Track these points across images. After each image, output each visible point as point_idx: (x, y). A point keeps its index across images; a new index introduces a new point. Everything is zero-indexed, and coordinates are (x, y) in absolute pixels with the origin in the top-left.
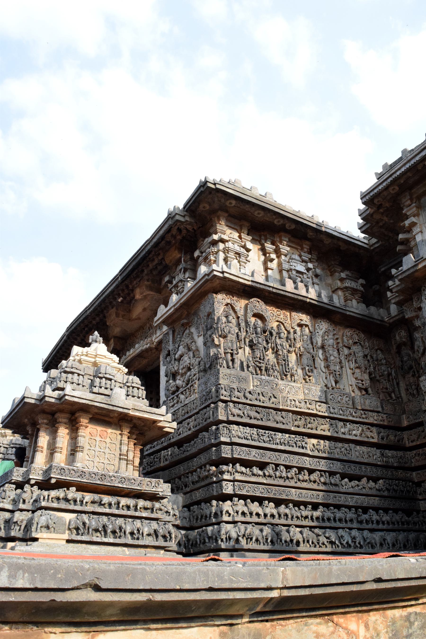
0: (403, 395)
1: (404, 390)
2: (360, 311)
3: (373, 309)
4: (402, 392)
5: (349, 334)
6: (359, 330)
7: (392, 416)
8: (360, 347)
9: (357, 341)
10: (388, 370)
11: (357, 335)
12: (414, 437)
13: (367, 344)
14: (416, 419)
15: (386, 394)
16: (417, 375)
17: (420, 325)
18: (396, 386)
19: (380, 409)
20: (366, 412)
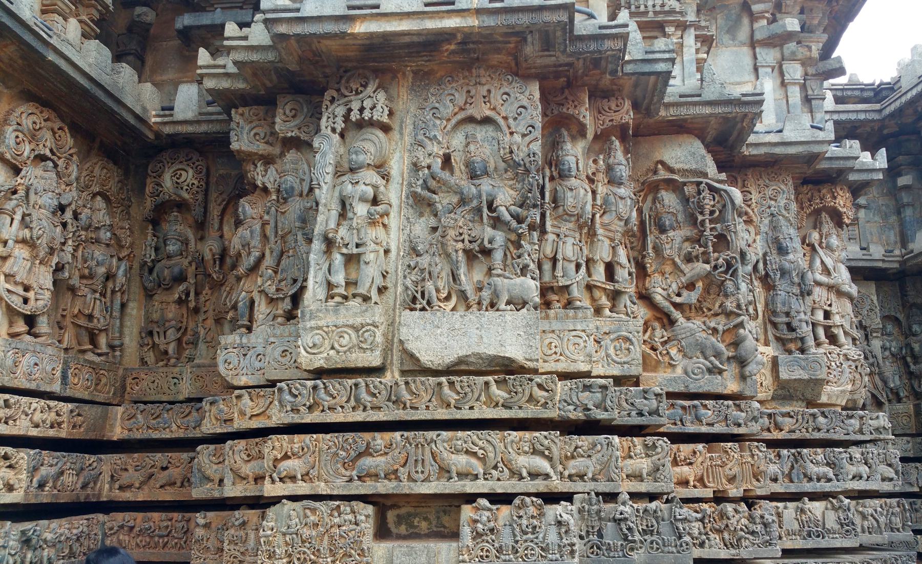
0: (127, 340)
1: (135, 331)
2: (90, 65)
3: (126, 72)
4: (126, 331)
5: (27, 122)
6: (63, 121)
7: (86, 407)
8: (54, 176)
9: (48, 153)
10: (110, 265)
11: (54, 133)
12: (132, 476)
13: (74, 170)
14: (156, 429)
15: (84, 332)
16: (192, 305)
17: (269, 186)
18: (116, 314)
19: (56, 387)
20: (13, 399)
